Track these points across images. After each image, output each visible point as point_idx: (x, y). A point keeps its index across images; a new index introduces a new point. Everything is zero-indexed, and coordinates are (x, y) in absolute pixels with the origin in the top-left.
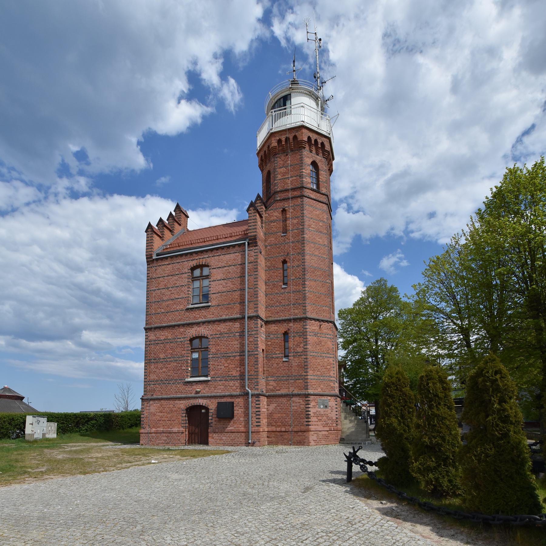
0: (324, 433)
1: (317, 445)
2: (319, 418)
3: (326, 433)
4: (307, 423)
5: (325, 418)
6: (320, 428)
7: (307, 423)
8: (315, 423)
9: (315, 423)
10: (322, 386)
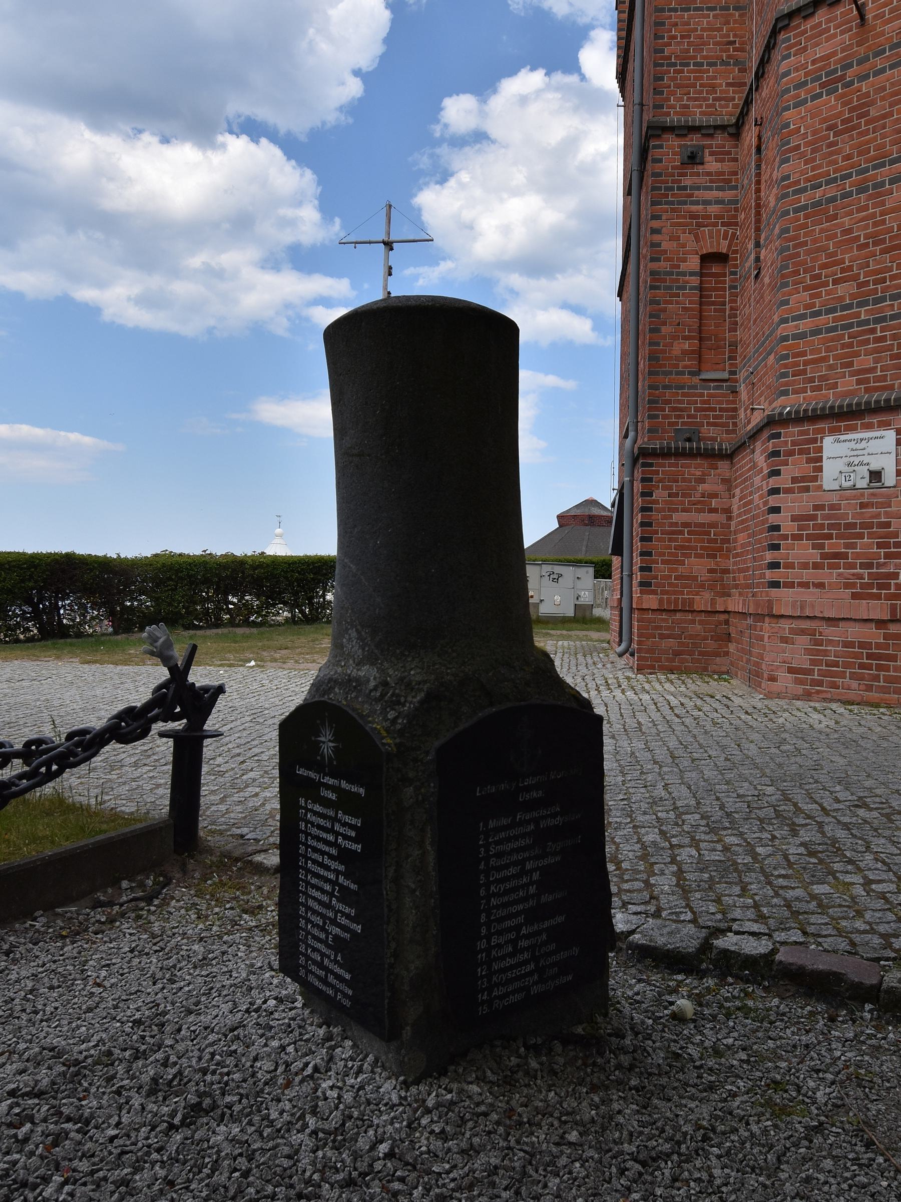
0: (854, 632)
1: (807, 696)
2: (834, 545)
3: (874, 635)
4: (769, 575)
5: (866, 544)
6: (833, 601)
7: (769, 575)
8: (807, 575)
9: (807, 575)
10: (864, 361)
